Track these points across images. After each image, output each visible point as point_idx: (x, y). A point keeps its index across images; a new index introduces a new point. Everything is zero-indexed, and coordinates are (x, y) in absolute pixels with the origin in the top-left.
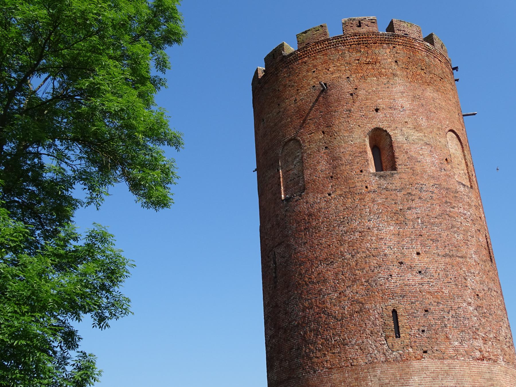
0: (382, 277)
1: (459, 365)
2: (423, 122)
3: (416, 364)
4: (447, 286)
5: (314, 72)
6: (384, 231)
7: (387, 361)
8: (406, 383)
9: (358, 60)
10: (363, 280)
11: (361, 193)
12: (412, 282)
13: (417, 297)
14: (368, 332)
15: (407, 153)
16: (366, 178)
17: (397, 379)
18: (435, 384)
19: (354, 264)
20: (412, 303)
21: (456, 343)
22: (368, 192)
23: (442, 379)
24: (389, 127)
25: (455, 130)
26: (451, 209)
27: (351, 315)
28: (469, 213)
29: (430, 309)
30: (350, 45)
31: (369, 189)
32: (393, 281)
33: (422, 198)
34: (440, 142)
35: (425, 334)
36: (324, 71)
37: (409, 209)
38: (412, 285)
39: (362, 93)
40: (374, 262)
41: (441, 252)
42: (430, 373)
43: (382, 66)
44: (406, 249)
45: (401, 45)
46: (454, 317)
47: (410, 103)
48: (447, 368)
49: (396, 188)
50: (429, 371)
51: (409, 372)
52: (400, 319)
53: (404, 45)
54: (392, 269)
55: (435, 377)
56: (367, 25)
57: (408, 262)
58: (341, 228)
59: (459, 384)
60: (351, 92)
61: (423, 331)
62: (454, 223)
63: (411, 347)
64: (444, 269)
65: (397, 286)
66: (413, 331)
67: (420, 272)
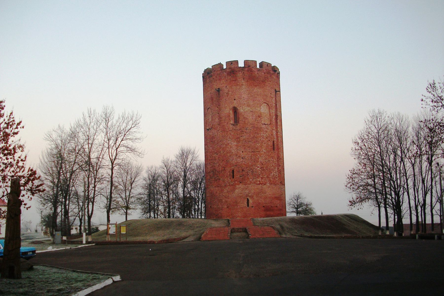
2: (251, 103)
3: (237, 186)
7: (230, 185)
14: (225, 176)
21: (251, 180)
25: (266, 102)
27: (221, 171)
34: (257, 110)
35: (241, 178)
37: (241, 136)
39: (230, 93)
40: (229, 155)
41: (250, 150)
53: (248, 71)
61: (241, 176)
62: (257, 140)
63: (237, 181)
67: (242, 158)
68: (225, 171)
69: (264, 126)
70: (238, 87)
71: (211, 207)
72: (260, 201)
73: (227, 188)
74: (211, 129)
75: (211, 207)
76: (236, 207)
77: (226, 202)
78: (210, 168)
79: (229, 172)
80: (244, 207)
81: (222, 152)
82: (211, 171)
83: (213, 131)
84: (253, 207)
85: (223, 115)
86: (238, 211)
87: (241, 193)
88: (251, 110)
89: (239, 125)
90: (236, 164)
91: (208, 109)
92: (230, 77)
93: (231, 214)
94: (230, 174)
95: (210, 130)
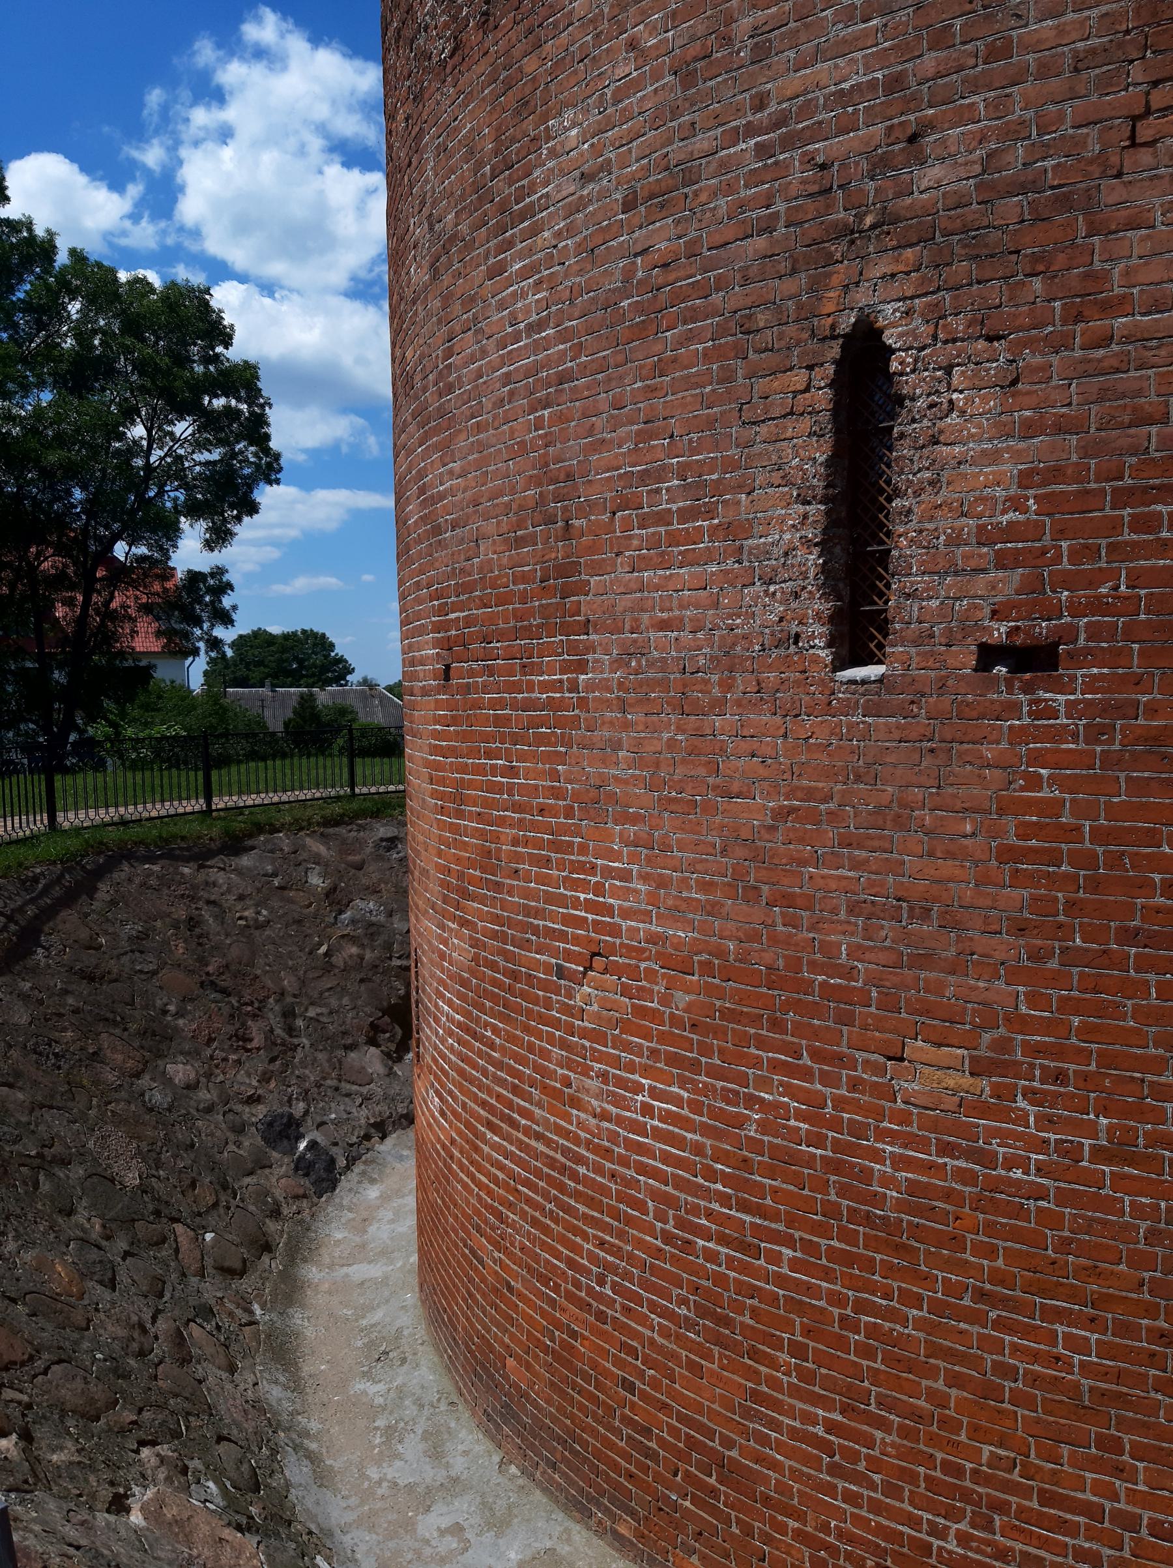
23: (761, 54)
80: (727, 662)
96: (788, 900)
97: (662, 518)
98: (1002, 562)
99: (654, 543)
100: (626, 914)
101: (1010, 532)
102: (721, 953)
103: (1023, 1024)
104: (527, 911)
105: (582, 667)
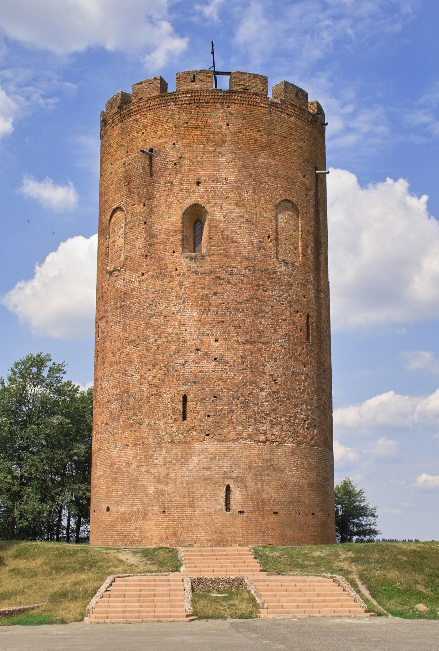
0: (179, 363)
1: (238, 448)
2: (248, 195)
3: (197, 446)
4: (241, 373)
5: (143, 133)
6: (187, 317)
7: (172, 442)
8: (186, 462)
9: (187, 123)
10: (162, 365)
11: (171, 276)
12: (206, 369)
13: (208, 384)
14: (160, 414)
15: (222, 232)
16: (177, 260)
17: (179, 458)
18: (211, 464)
19: (156, 348)
20: (203, 389)
22: (178, 275)
23: (219, 460)
24: (208, 203)
25: (290, 198)
26: (263, 293)
27: (148, 398)
28: (286, 294)
29: (219, 395)
30: (181, 104)
31: (178, 272)
32: (188, 367)
33: (231, 283)
35: (211, 419)
36: (152, 134)
37: (215, 294)
38: (206, 372)
42: (209, 454)
43: (212, 130)
44: (206, 335)
45: (237, 103)
46: (243, 403)
47: (236, 175)
48: (225, 450)
49: (205, 271)
50: (208, 452)
51: (189, 452)
52: (189, 403)
54: (189, 356)
55: (213, 458)
56: (201, 80)
57: (204, 349)
58: (149, 311)
59: (235, 464)
60: (176, 162)
61: (209, 416)
62: (264, 308)
63: (196, 430)
64: (241, 356)
65: (191, 372)
66: (199, 416)
67: (215, 359)
68: (160, 396)
69: (284, 268)
70: (210, 147)
71: (108, 509)
72: (264, 495)
73: (164, 451)
74: (119, 271)
75: (108, 509)
76: (190, 511)
77: (160, 493)
78: (113, 388)
79: (173, 402)
80: (215, 511)
81: (152, 340)
82: (115, 397)
83: (127, 275)
84: (242, 512)
85: (160, 227)
86: (196, 525)
87: (208, 469)
88: (246, 216)
89: (208, 258)
90: (196, 377)
91: (115, 211)
92: (185, 116)
93: (174, 534)
94: (174, 408)
95: (116, 273)
96: (222, 533)
97: (208, 498)
98: (240, 505)
99: (206, 500)
100: (201, 537)
101: (240, 502)
102: (214, 539)
103: (242, 541)
104: (184, 539)
105: (195, 511)
